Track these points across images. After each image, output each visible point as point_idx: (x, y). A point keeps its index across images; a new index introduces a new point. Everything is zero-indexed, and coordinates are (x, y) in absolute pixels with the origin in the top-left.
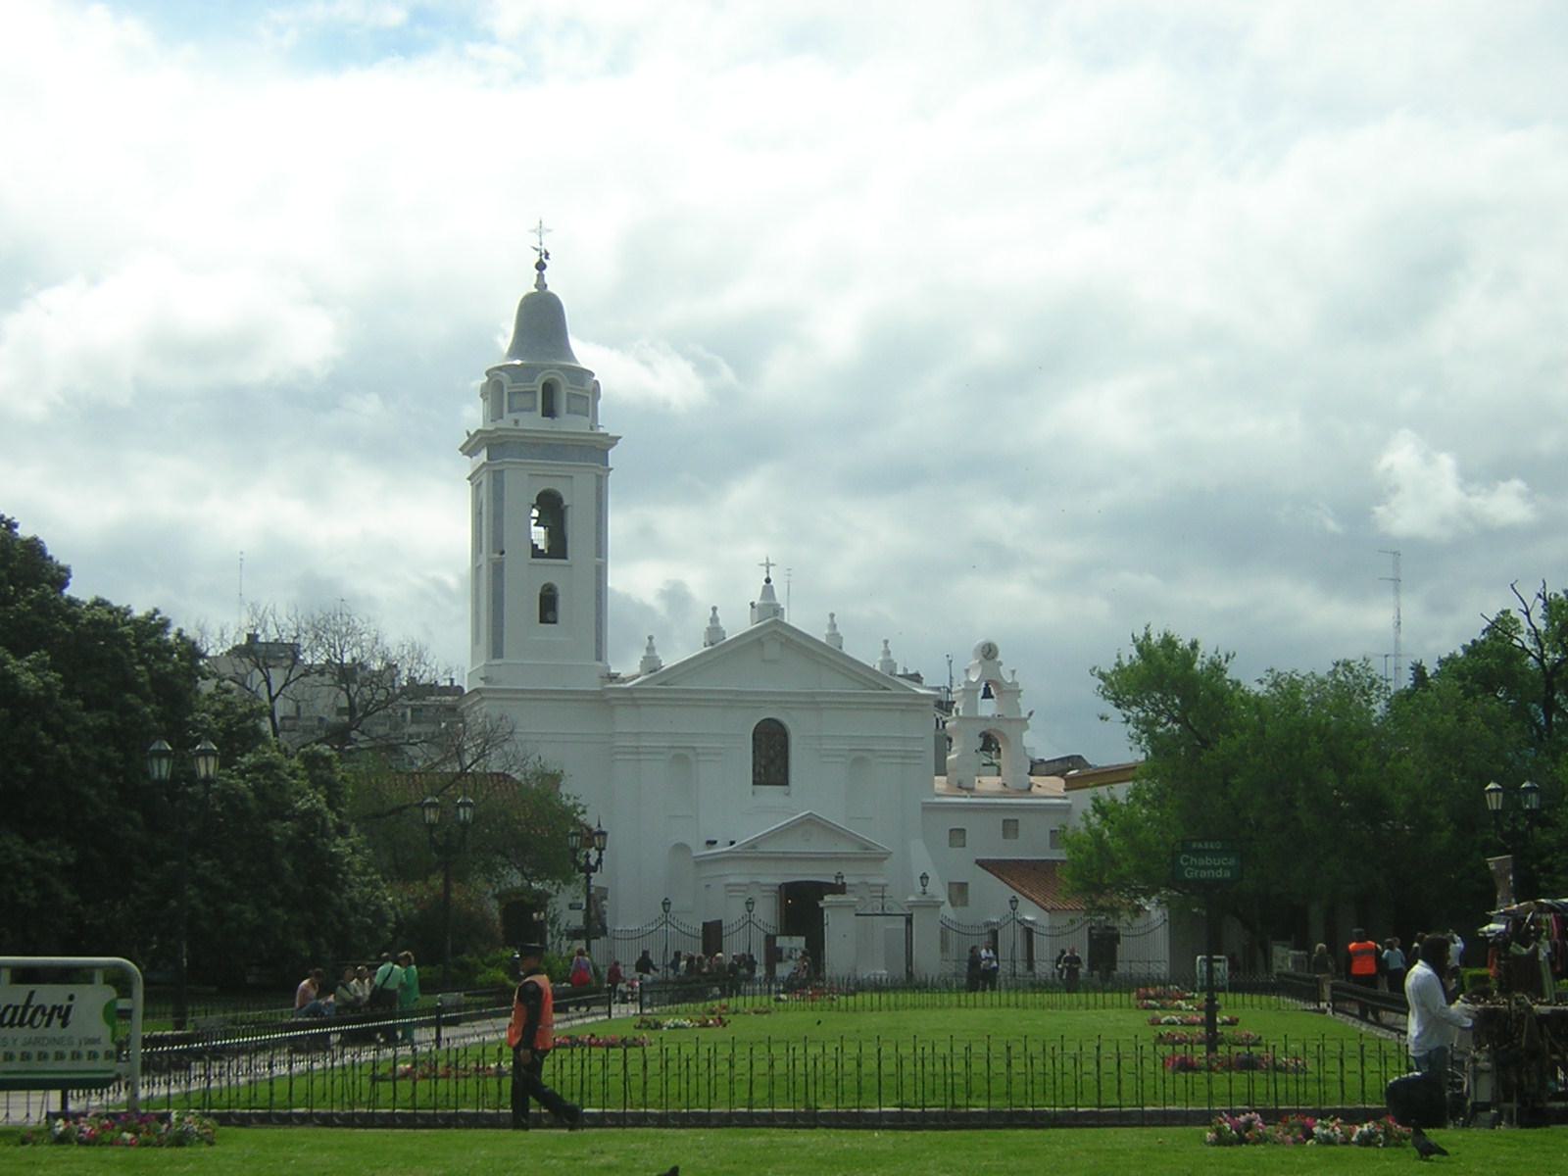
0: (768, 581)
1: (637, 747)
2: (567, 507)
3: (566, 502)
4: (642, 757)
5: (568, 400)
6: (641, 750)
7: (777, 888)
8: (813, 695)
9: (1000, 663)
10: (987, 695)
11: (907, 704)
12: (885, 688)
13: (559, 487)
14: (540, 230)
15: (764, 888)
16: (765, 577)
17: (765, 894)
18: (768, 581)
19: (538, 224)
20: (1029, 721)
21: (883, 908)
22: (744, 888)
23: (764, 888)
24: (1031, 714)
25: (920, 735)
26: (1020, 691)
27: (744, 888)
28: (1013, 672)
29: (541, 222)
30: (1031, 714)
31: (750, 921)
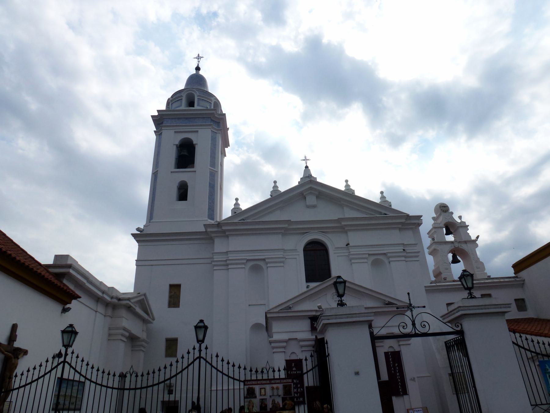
0: (307, 167)
1: (226, 261)
2: (195, 144)
3: (194, 143)
4: (230, 267)
5: (198, 101)
6: (228, 262)
7: (313, 343)
8: (339, 220)
9: (452, 213)
10: (448, 233)
11: (402, 224)
12: (386, 214)
13: (193, 137)
14: (199, 57)
15: (302, 343)
16: (305, 165)
17: (304, 349)
18: (307, 167)
19: (197, 56)
20: (477, 242)
21: (414, 324)
22: (285, 344)
23: (302, 343)
24: (478, 237)
25: (414, 243)
26: (468, 226)
27: (285, 344)
28: (460, 217)
29: (199, 55)
30: (478, 237)
31: (200, 357)
